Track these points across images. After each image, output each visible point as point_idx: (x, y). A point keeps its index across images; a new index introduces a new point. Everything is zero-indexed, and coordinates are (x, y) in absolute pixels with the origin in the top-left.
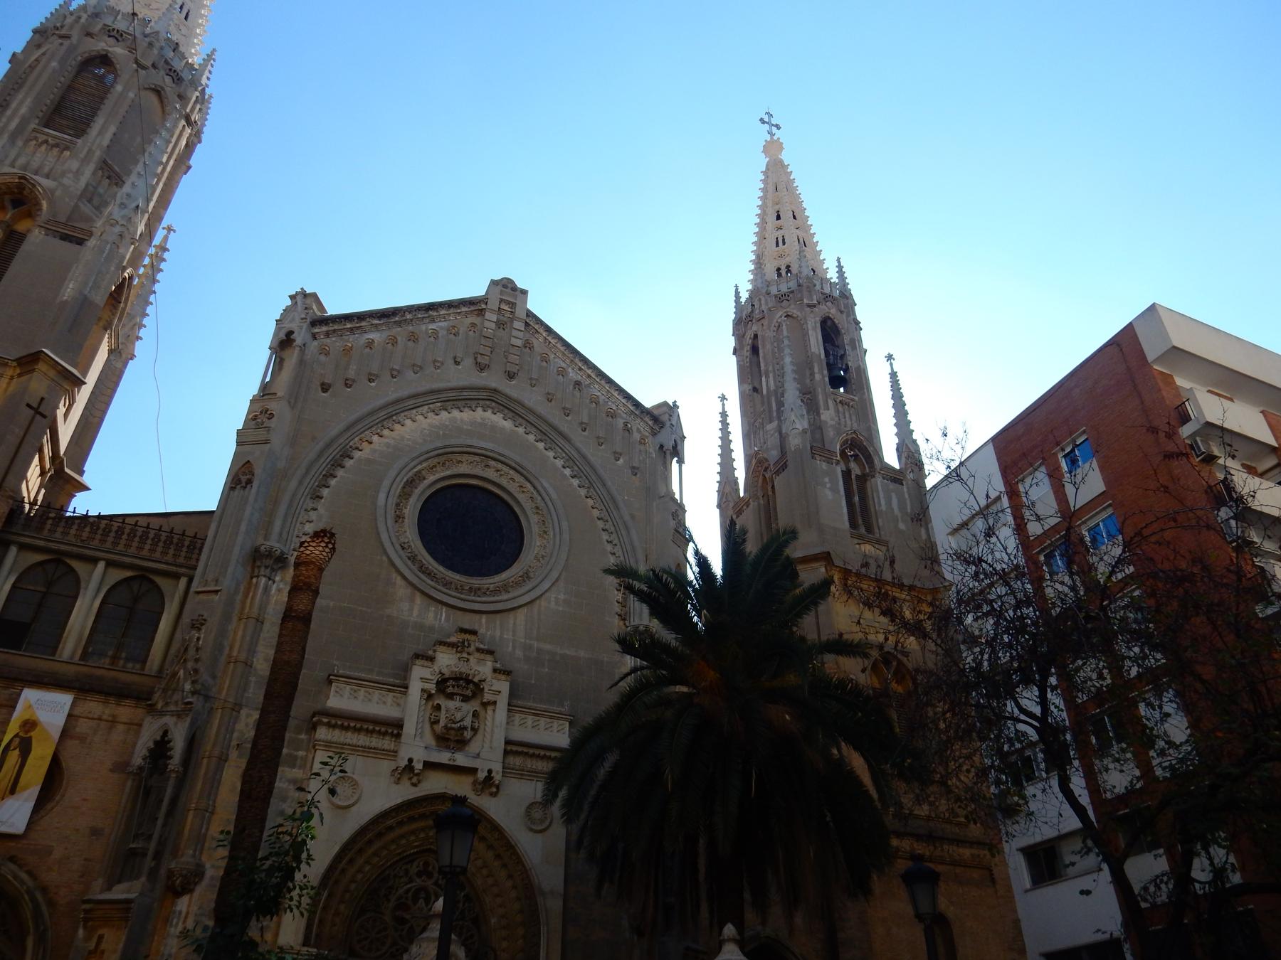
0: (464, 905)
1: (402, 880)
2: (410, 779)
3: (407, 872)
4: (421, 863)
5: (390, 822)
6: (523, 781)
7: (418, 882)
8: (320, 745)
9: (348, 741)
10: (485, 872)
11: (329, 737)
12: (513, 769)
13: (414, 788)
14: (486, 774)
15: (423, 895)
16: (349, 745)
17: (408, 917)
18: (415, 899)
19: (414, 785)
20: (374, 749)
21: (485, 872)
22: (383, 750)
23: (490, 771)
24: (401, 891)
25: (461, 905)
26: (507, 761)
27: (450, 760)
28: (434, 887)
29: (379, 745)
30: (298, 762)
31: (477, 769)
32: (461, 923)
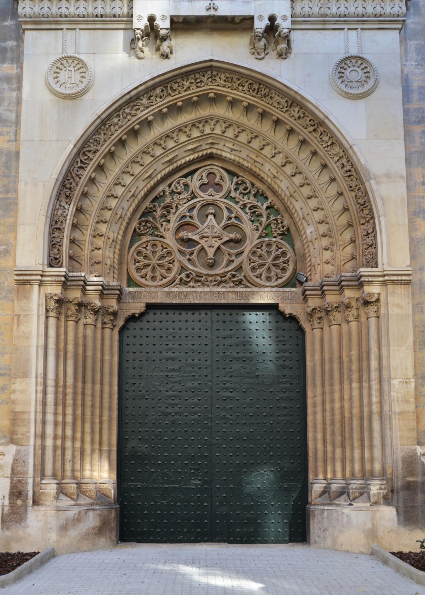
0: (268, 218)
1: (182, 196)
2: (158, 49)
3: (186, 186)
4: (204, 174)
5: (142, 114)
6: (326, 32)
7: (203, 196)
8: (26, 22)
9: (64, 11)
10: (289, 169)
11: (37, 9)
12: (309, 16)
13: (166, 60)
14: (266, 22)
15: (211, 210)
16: (66, 16)
17: (196, 238)
18: (204, 217)
19: (165, 56)
20: (102, 16)
21: (289, 169)
22: (114, 16)
23: (272, 19)
24: (183, 209)
25: (264, 219)
26: (298, 10)
27: (208, 9)
28: (226, 201)
29: (108, 10)
30: (9, 55)
31: (252, 18)
32: (266, 239)
